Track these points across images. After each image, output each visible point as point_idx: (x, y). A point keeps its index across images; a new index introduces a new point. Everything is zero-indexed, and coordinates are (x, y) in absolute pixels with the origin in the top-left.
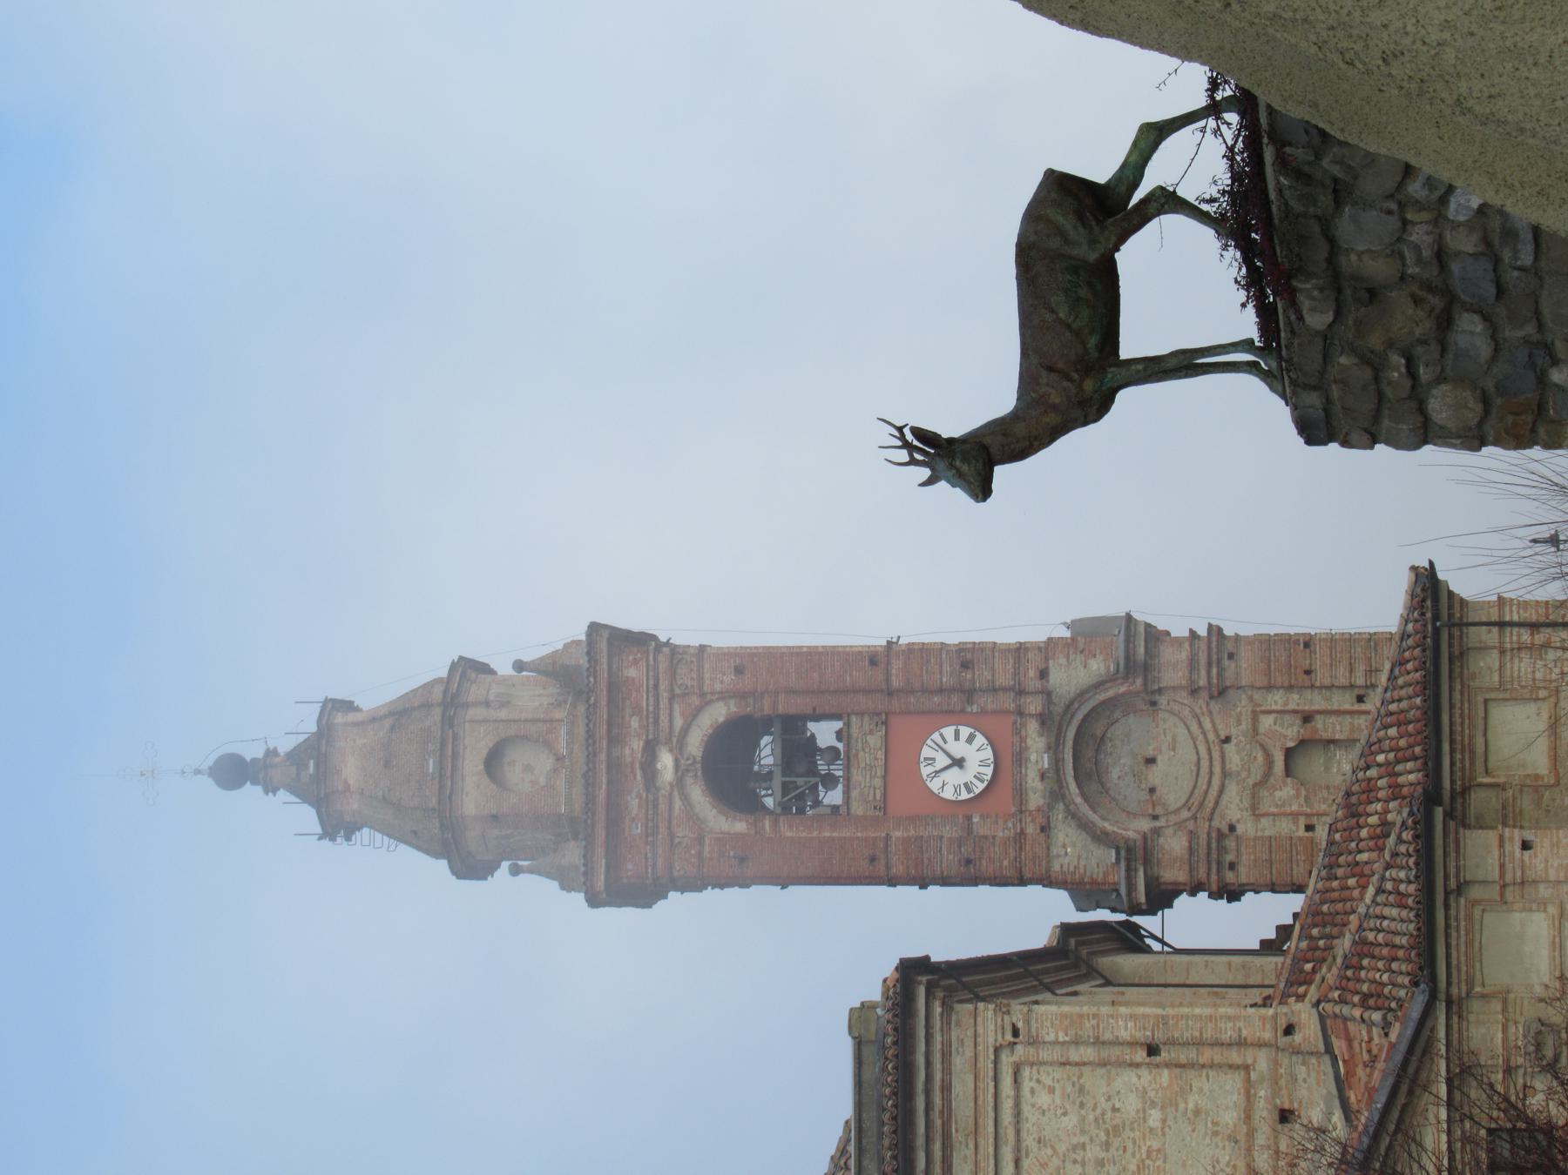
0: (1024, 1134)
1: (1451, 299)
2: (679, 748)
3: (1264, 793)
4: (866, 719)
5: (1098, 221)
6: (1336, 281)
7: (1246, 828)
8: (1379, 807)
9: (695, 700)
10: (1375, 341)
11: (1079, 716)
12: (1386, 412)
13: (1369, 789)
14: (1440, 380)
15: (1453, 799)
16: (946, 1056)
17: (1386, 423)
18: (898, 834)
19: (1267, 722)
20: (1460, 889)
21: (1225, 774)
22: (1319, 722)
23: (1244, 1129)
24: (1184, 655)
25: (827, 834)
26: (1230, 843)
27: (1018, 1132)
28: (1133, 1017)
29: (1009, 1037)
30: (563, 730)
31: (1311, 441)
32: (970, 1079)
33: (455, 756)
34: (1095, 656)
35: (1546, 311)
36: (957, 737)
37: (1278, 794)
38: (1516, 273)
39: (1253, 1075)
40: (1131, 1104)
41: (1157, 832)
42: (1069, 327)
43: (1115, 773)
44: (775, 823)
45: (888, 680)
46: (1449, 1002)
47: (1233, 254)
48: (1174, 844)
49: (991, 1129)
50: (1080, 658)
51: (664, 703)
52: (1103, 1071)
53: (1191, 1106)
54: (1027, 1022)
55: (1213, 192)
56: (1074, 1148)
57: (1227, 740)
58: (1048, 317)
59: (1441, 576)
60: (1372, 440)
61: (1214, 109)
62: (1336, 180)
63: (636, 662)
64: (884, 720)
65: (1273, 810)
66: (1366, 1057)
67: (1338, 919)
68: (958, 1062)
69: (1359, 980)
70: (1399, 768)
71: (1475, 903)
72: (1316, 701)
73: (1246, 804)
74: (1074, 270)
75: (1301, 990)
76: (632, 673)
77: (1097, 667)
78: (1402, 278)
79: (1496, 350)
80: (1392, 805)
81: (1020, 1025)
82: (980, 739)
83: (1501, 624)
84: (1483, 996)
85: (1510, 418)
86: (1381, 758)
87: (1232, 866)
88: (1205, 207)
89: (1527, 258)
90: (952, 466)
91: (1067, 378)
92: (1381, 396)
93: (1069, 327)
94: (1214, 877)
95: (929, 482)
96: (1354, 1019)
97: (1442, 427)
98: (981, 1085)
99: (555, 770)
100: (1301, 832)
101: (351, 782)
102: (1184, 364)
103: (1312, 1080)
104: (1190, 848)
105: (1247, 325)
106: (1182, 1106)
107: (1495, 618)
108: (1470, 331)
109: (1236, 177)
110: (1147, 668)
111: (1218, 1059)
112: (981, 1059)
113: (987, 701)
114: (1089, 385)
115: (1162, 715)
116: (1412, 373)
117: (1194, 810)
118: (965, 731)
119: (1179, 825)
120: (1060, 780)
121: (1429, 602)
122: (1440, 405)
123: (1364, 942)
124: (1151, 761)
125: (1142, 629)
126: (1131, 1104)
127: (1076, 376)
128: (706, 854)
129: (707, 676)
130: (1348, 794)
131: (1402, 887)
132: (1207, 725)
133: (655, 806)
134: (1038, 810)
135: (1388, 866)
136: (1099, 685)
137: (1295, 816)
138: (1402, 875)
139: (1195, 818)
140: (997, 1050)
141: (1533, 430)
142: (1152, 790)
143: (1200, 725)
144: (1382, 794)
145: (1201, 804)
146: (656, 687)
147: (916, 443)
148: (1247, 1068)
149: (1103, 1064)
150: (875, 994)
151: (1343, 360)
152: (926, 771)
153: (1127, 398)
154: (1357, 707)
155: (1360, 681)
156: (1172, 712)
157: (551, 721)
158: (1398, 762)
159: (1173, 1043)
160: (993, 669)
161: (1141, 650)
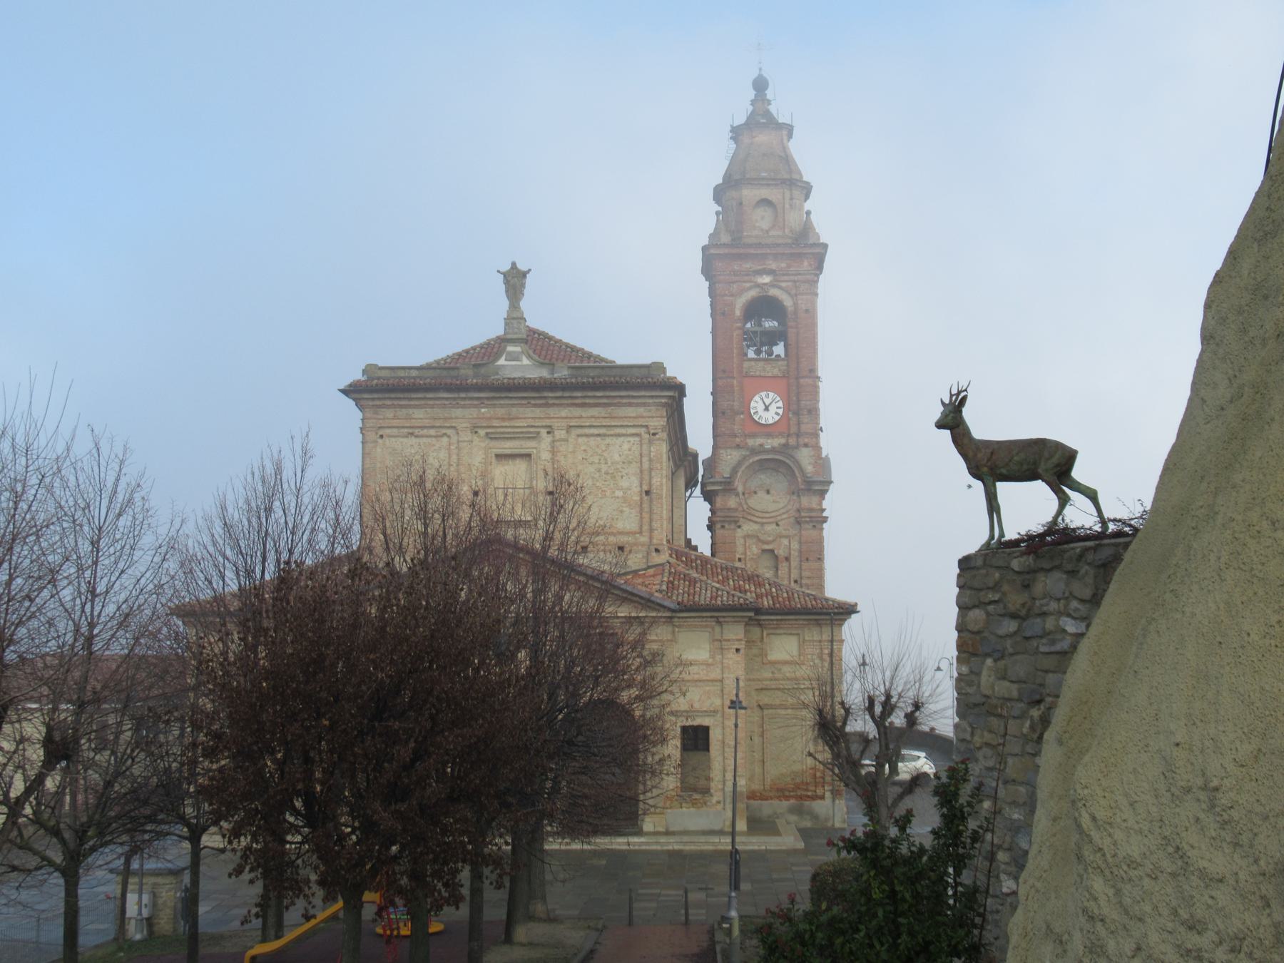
0: (611, 438)
1: (1024, 619)
2: (772, 285)
3: (754, 540)
4: (785, 368)
5: (1055, 473)
6: (1033, 571)
7: (739, 533)
8: (753, 589)
9: (793, 292)
10: (1006, 587)
11: (787, 461)
12: (973, 592)
13: (760, 585)
14: (988, 614)
15: (757, 620)
16: (644, 405)
17: (968, 592)
18: (735, 382)
19: (785, 542)
20: (719, 623)
21: (762, 524)
22: (785, 564)
23: (615, 531)
24: (814, 506)
25: (735, 351)
26: (733, 526)
27: (612, 435)
28: (662, 484)
29: (652, 432)
30: (780, 233)
31: (960, 561)
32: (634, 415)
33: (768, 185)
35: (1018, 657)
36: (778, 408)
37: (754, 546)
38: (1035, 645)
39: (638, 535)
40: (624, 484)
41: (737, 495)
42: (1010, 461)
43: (763, 477)
44: (739, 328)
45: (803, 377)
46: (671, 618)
47: (1041, 530)
48: (732, 502)
49: (613, 424)
51: (792, 278)
52: (639, 471)
53: (624, 509)
54: (659, 439)
55: (1067, 520)
56: (606, 459)
57: (778, 525)
58: (1014, 452)
59: (853, 616)
60: (961, 586)
61: (1104, 522)
62: (1078, 571)
63: (810, 265)
64: (785, 376)
65: (747, 544)
66: (647, 583)
67: (704, 571)
68: (641, 410)
69: (679, 580)
70: (769, 597)
71: (713, 630)
72: (794, 563)
73: (750, 533)
74: (1035, 463)
75: (674, 556)
76: (806, 263)
77: (809, 469)
78: (1034, 599)
79: (1001, 637)
80: (754, 595)
81: (657, 436)
82: (777, 418)
83: (832, 641)
84: (674, 632)
85: (970, 642)
86: (774, 590)
87: (723, 527)
88: (1060, 518)
89: (1043, 649)
90: (950, 412)
91: (988, 460)
92: (981, 590)
93: (1010, 461)
94: (718, 519)
95: (943, 403)
96: (663, 577)
97: (967, 615)
98: (631, 420)
99: (762, 230)
100: (738, 556)
101: (757, 139)
102: (993, 507)
103: (636, 560)
104: (729, 509)
105: (1010, 535)
106: (624, 505)
107: (835, 638)
108: (1011, 626)
109: (1074, 530)
110: (809, 490)
111: (644, 521)
112: (643, 420)
113: (794, 421)
114: (985, 469)
115: (788, 496)
116: (991, 603)
118: (781, 411)
119: (740, 504)
120: (760, 453)
121: (841, 611)
122: (977, 615)
123: (695, 582)
124: (768, 492)
125: (826, 488)
126: (624, 484)
127: (989, 464)
128: (725, 298)
129: (804, 297)
130: (758, 576)
131: (719, 598)
132: (784, 516)
133: (747, 275)
134: (746, 444)
135: (728, 593)
136: (801, 470)
137: (745, 554)
138: (725, 598)
139: (744, 511)
140: (647, 426)
141: (965, 652)
142: (755, 493)
143: (784, 513)
144: (758, 590)
145: (750, 514)
146: (800, 274)
147: (960, 397)
148: (641, 533)
149: (641, 472)
150: (669, 374)
151: (997, 575)
152: (763, 394)
153: (978, 486)
154: (792, 580)
155: (803, 582)
156: (789, 501)
157: (784, 228)
158: (772, 597)
159: (651, 501)
160: (807, 423)
161: (817, 488)
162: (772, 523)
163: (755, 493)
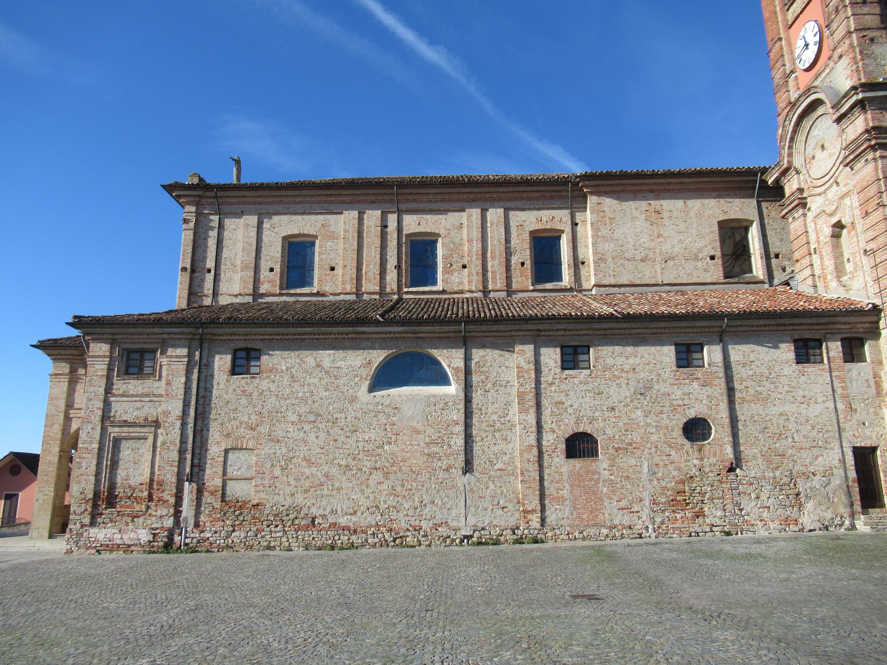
19: (847, 201)
26: (801, 211)
34: (851, 79)
50: (848, 72)
72: (859, 227)
115: (840, 139)
117: (812, 185)
118: (817, 38)
137: (818, 242)
162: (831, 186)
163: (813, 157)
